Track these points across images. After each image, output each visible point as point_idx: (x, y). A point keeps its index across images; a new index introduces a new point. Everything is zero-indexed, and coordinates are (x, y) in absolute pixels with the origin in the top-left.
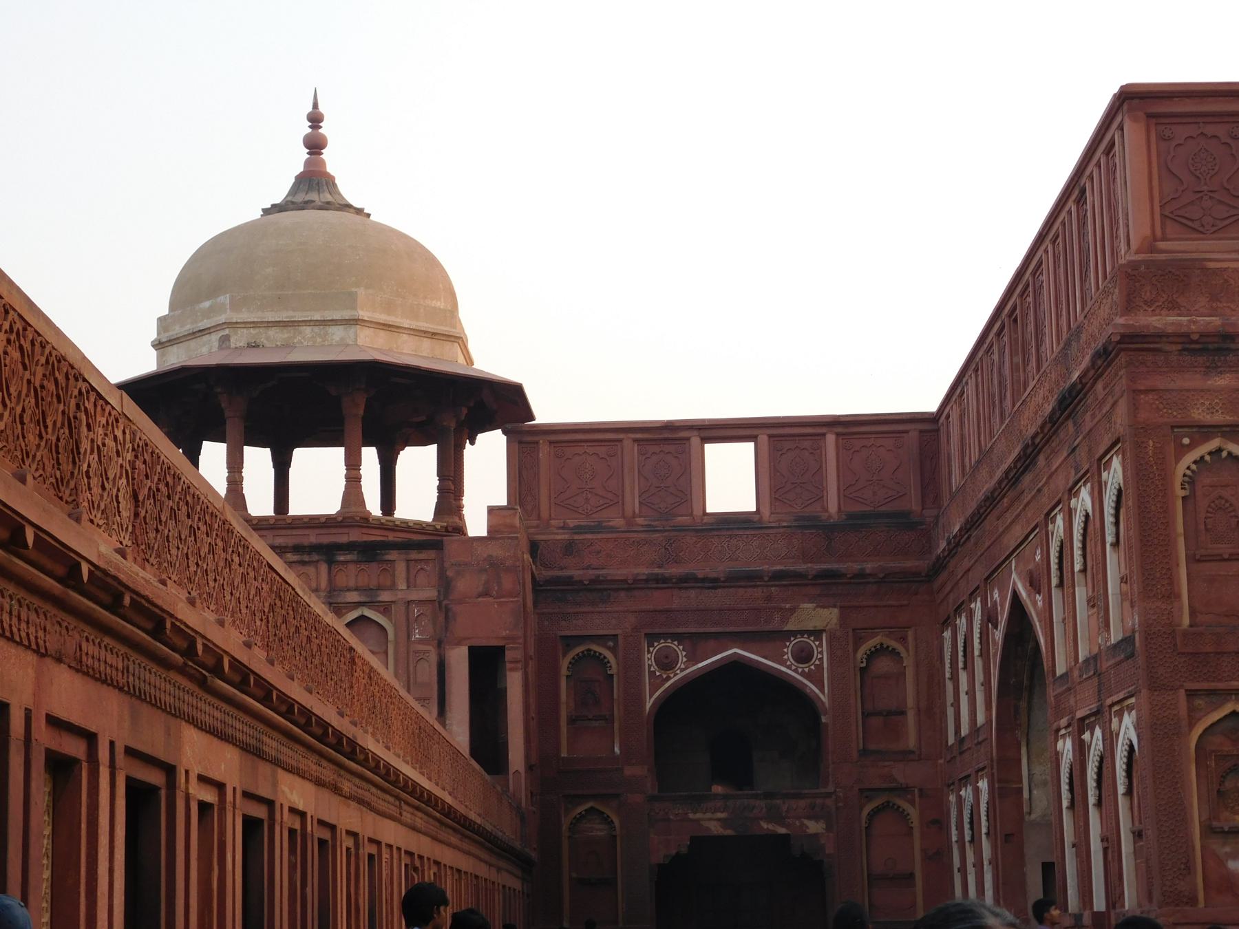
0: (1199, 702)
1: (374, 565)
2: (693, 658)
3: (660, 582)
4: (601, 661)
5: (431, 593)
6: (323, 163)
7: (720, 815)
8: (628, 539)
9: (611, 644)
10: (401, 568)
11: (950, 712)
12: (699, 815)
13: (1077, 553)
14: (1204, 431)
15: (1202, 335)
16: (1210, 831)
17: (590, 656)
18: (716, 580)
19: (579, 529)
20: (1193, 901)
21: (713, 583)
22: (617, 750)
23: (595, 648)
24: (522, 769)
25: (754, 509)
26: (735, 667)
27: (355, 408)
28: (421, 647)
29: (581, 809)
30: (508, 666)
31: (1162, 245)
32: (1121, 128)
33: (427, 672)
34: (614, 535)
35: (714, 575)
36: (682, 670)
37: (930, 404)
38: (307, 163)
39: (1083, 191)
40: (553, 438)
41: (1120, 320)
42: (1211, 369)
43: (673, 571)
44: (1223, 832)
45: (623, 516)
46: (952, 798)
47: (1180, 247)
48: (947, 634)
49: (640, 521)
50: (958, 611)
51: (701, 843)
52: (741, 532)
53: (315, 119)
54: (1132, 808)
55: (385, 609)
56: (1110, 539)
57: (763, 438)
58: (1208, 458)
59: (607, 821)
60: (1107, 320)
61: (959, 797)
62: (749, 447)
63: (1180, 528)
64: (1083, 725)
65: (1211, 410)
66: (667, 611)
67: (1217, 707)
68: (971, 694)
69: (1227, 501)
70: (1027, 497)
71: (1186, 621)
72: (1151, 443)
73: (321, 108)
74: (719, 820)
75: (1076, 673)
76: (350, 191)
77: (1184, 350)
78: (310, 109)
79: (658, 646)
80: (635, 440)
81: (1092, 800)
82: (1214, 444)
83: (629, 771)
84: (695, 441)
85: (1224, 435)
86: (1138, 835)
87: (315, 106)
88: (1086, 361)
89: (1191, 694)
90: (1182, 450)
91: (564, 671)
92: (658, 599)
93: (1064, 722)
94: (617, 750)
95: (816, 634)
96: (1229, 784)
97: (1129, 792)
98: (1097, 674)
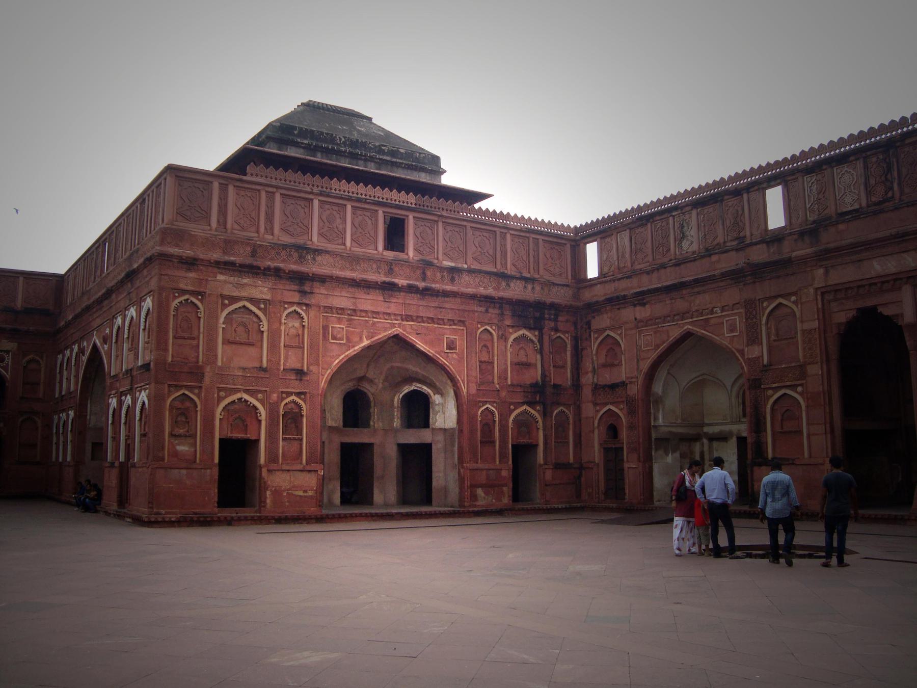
0: (172, 389)
11: (58, 385)
13: (126, 331)
14: (183, 292)
16: (172, 435)
20: (163, 459)
31: (176, 223)
32: (165, 179)
37: (62, 271)
39: (144, 200)
41: (158, 248)
42: (189, 270)
46: (56, 417)
47: (183, 225)
48: (60, 356)
50: (66, 348)
54: (141, 425)
56: (142, 327)
60: (153, 247)
61: (59, 418)
64: (123, 394)
67: (178, 391)
68: (68, 379)
70: (104, 309)
71: (170, 359)
75: (121, 375)
81: (123, 421)
82: (186, 297)
85: (190, 294)
86: (143, 435)
88: (141, 261)
89: (170, 386)
90: (175, 298)
93: (113, 392)
95: (7, 352)
96: (179, 419)
97: (140, 420)
98: (132, 376)
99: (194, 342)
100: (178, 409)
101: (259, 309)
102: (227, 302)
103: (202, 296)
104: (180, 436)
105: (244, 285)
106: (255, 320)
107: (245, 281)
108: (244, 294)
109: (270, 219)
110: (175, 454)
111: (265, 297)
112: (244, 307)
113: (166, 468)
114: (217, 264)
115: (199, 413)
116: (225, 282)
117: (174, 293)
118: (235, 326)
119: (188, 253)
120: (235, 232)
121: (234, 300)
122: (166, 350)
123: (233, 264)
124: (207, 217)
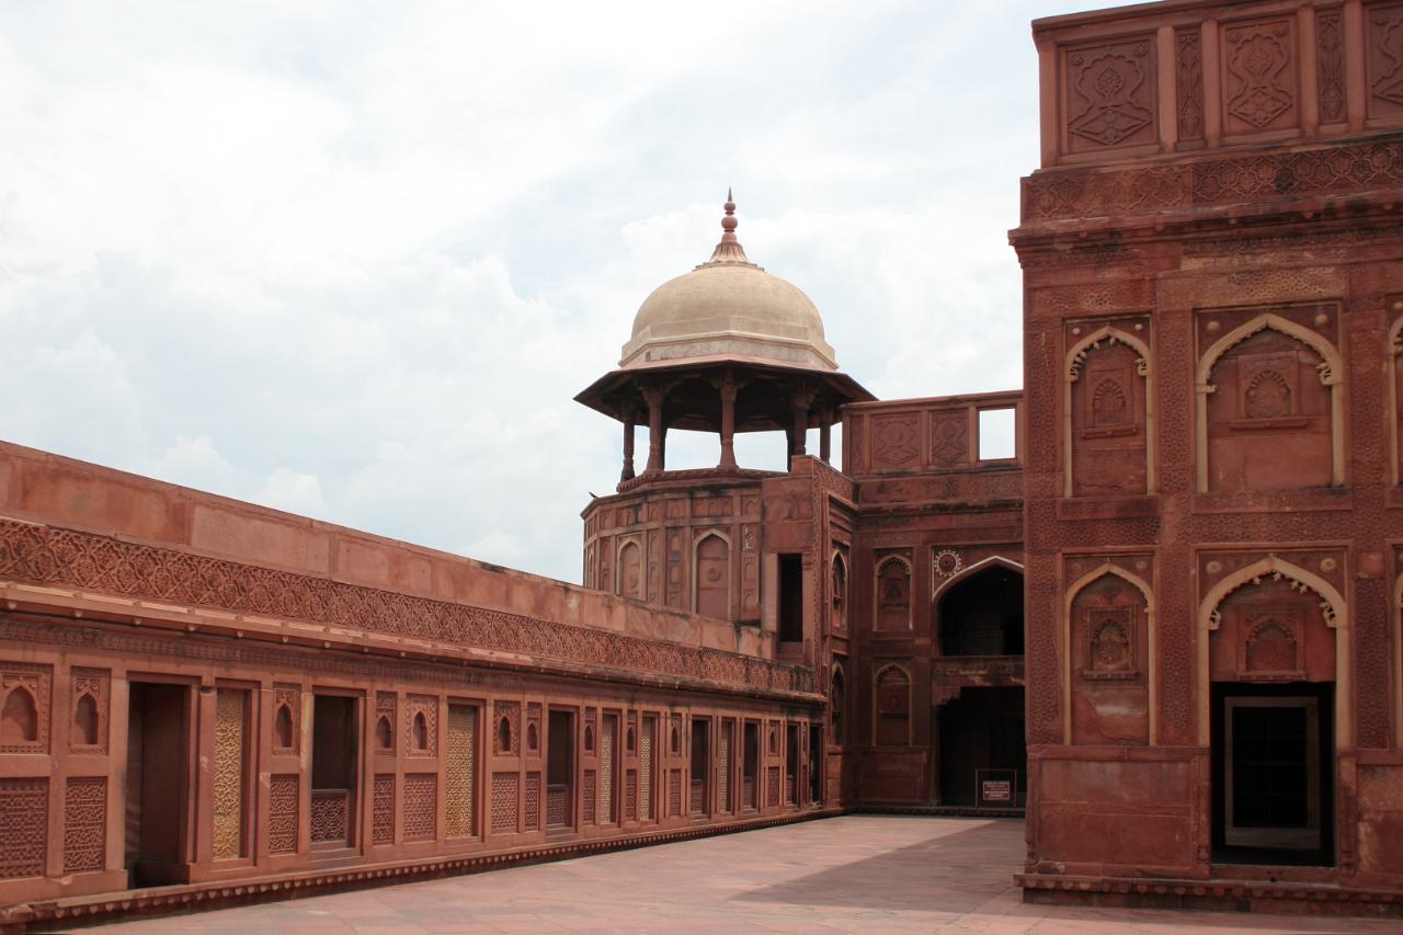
1: (719, 500)
2: (966, 563)
3: (943, 510)
4: (903, 566)
5: (756, 518)
6: (735, 238)
7: (981, 672)
8: (920, 480)
9: (908, 554)
10: (737, 500)
12: (967, 672)
14: (1094, 322)
15: (1091, 233)
17: (893, 562)
18: (981, 507)
19: (891, 475)
21: (979, 509)
22: (911, 626)
23: (898, 557)
24: (813, 638)
25: (1013, 456)
26: (997, 570)
27: (729, 395)
28: (752, 555)
29: (886, 667)
30: (804, 567)
33: (752, 570)
34: (910, 478)
35: (980, 504)
36: (958, 571)
38: (724, 238)
40: (874, 412)
42: (1101, 264)
43: (952, 501)
44: (1093, 680)
45: (921, 465)
49: (932, 467)
51: (969, 692)
52: (1000, 473)
53: (730, 209)
55: (727, 530)
57: (1021, 405)
58: (1097, 345)
59: (906, 676)
62: (1010, 413)
63: (1068, 410)
65: (1100, 301)
66: (949, 530)
69: (1115, 384)
71: (1069, 493)
72: (1044, 335)
73: (734, 201)
74: (980, 675)
76: (751, 254)
77: (1076, 248)
78: (726, 201)
79: (941, 554)
80: (930, 411)
83: (918, 642)
84: (972, 409)
85: (1113, 324)
87: (730, 199)
89: (1068, 558)
90: (1071, 341)
91: (876, 573)
92: (942, 522)
94: (911, 626)
96: (1103, 637)
99: (1134, 443)
100: (1101, 613)
101: (1312, 326)
102: (1213, 325)
103: (1145, 322)
104: (1102, 680)
105: (1258, 274)
106: (1306, 359)
107: (1264, 260)
108: (1262, 294)
109: (1331, 78)
110: (1096, 725)
111: (1325, 292)
112: (1267, 329)
113: (1066, 760)
114: (1176, 229)
115: (1152, 622)
116: (1206, 274)
117: (1068, 331)
118: (1245, 384)
119: (1091, 218)
120: (1228, 140)
121: (1232, 316)
122: (1055, 469)
123: (1220, 222)
124: (1145, 123)
